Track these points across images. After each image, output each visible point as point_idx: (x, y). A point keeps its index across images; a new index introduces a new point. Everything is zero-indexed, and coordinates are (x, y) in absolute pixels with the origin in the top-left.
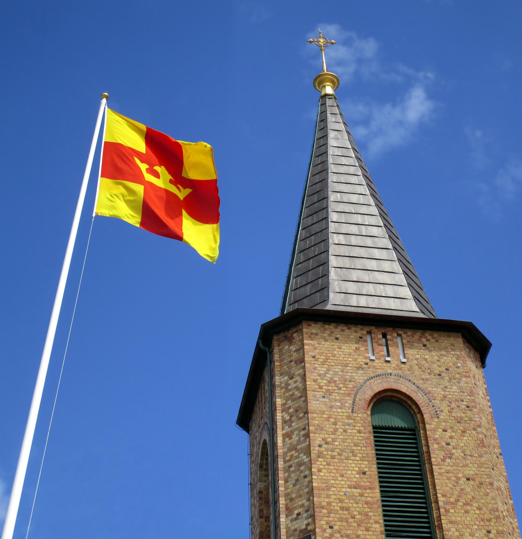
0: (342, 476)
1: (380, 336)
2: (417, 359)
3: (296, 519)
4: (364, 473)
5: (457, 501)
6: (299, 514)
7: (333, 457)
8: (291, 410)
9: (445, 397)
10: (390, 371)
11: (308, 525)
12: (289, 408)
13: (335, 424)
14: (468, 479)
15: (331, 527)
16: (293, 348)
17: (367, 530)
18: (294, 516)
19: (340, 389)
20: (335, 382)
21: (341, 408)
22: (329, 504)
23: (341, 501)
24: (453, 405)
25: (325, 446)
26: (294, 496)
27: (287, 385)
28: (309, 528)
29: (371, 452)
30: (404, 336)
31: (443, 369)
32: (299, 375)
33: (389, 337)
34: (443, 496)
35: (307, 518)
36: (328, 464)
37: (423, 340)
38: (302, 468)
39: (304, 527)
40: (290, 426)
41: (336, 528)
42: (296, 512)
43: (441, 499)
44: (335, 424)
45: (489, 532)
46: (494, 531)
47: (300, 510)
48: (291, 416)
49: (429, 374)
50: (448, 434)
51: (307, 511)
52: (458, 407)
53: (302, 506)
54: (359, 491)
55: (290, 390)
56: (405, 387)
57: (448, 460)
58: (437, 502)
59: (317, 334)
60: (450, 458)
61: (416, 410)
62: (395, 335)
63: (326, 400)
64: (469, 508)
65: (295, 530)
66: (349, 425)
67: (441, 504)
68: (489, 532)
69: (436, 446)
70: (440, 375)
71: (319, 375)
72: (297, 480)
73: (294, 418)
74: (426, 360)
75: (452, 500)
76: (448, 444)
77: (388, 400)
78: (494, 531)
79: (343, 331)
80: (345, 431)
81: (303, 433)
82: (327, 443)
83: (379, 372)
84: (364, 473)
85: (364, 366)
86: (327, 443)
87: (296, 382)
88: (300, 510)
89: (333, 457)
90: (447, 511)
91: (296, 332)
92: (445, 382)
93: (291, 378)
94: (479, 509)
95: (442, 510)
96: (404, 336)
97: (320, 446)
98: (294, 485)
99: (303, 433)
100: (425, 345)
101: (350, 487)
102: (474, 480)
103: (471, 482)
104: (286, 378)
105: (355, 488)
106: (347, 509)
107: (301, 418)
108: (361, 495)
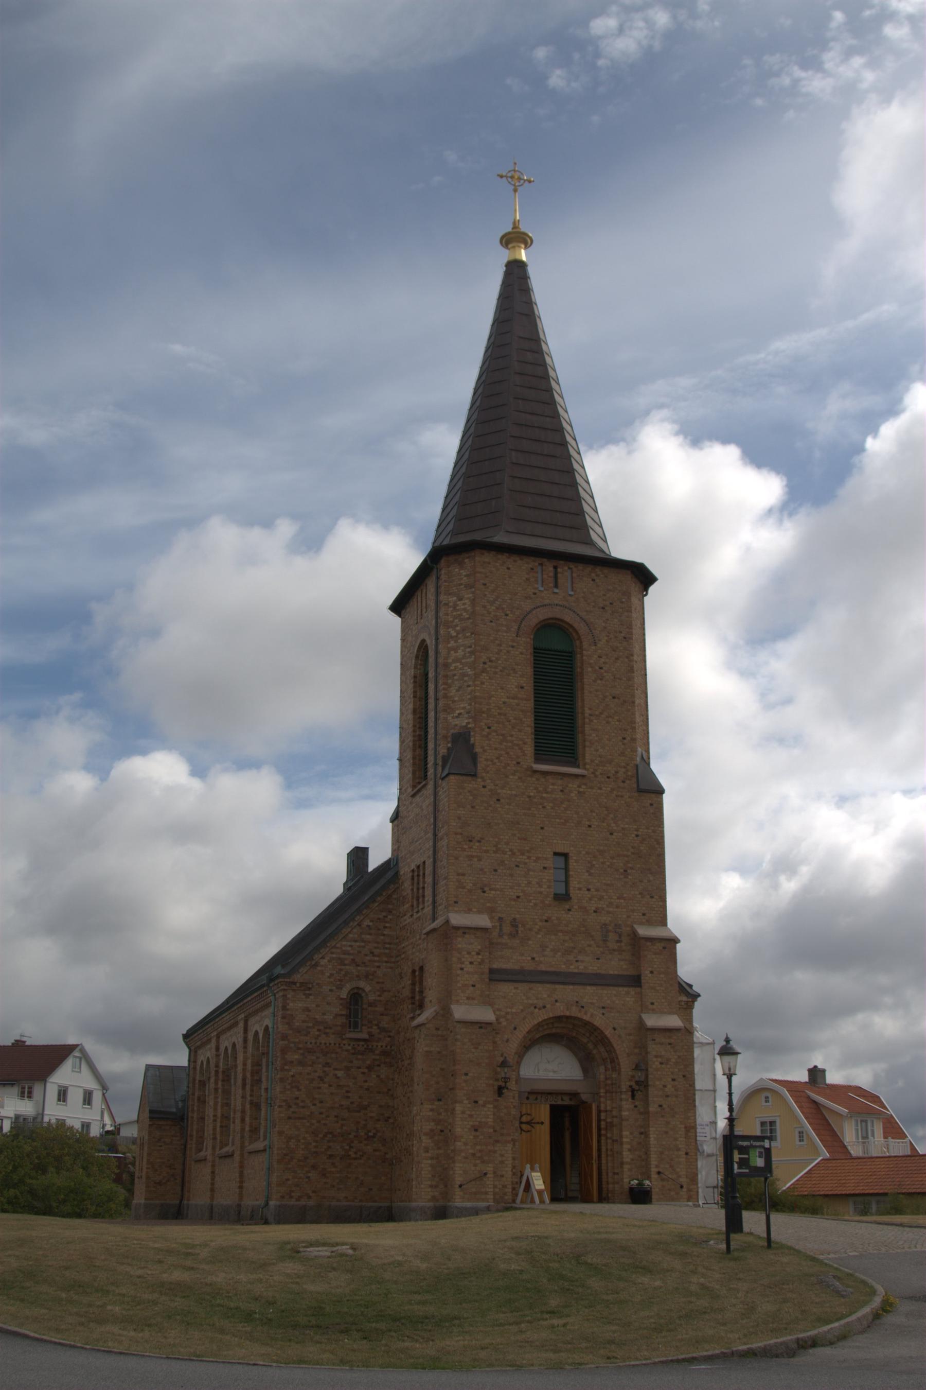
0: (502, 688)
1: (551, 569)
2: (584, 593)
3: (457, 717)
4: (522, 688)
5: (601, 713)
6: (460, 714)
7: (496, 673)
8: (458, 628)
9: (605, 628)
10: (556, 602)
11: (468, 723)
12: (457, 626)
13: (500, 645)
14: (614, 698)
15: (489, 728)
16: (463, 572)
17: (520, 731)
18: (456, 715)
19: (507, 615)
20: (503, 609)
21: (506, 632)
23: (500, 708)
24: (611, 636)
25: (489, 663)
26: (456, 699)
27: (455, 606)
28: (469, 726)
29: (529, 671)
30: (575, 569)
32: (467, 598)
33: (559, 570)
34: (590, 709)
35: (467, 718)
36: (490, 678)
37: (593, 575)
38: (466, 678)
39: (464, 724)
40: (456, 642)
41: (493, 728)
42: (458, 712)
43: (587, 711)
44: (500, 645)
45: (624, 739)
46: (628, 739)
47: (462, 711)
48: (458, 634)
49: (594, 607)
50: (603, 660)
51: (468, 713)
52: (616, 637)
53: (464, 708)
54: (516, 701)
55: (458, 610)
56: (568, 617)
57: (599, 682)
58: (583, 713)
59: (489, 563)
60: (601, 680)
61: (576, 637)
62: (566, 568)
63: (493, 624)
64: (610, 719)
65: (456, 725)
66: (513, 647)
67: (587, 715)
68: (624, 739)
69: (590, 669)
70: (603, 608)
72: (460, 687)
73: (460, 636)
74: (592, 593)
75: (597, 713)
76: (601, 668)
77: (552, 627)
78: (628, 739)
79: (515, 561)
80: (508, 652)
81: (469, 650)
82: (491, 661)
83: (547, 602)
84: (522, 688)
85: (533, 596)
86: (491, 661)
87: (464, 604)
88: (462, 711)
89: (496, 673)
90: (591, 721)
91: (468, 558)
93: (460, 600)
94: (619, 721)
95: (587, 720)
96: (575, 569)
97: (485, 663)
98: (458, 691)
99: (469, 650)
100: (593, 580)
101: (508, 698)
102: (619, 698)
103: (616, 700)
104: (455, 598)
105: (513, 698)
106: (505, 715)
107: (468, 637)
108: (518, 705)
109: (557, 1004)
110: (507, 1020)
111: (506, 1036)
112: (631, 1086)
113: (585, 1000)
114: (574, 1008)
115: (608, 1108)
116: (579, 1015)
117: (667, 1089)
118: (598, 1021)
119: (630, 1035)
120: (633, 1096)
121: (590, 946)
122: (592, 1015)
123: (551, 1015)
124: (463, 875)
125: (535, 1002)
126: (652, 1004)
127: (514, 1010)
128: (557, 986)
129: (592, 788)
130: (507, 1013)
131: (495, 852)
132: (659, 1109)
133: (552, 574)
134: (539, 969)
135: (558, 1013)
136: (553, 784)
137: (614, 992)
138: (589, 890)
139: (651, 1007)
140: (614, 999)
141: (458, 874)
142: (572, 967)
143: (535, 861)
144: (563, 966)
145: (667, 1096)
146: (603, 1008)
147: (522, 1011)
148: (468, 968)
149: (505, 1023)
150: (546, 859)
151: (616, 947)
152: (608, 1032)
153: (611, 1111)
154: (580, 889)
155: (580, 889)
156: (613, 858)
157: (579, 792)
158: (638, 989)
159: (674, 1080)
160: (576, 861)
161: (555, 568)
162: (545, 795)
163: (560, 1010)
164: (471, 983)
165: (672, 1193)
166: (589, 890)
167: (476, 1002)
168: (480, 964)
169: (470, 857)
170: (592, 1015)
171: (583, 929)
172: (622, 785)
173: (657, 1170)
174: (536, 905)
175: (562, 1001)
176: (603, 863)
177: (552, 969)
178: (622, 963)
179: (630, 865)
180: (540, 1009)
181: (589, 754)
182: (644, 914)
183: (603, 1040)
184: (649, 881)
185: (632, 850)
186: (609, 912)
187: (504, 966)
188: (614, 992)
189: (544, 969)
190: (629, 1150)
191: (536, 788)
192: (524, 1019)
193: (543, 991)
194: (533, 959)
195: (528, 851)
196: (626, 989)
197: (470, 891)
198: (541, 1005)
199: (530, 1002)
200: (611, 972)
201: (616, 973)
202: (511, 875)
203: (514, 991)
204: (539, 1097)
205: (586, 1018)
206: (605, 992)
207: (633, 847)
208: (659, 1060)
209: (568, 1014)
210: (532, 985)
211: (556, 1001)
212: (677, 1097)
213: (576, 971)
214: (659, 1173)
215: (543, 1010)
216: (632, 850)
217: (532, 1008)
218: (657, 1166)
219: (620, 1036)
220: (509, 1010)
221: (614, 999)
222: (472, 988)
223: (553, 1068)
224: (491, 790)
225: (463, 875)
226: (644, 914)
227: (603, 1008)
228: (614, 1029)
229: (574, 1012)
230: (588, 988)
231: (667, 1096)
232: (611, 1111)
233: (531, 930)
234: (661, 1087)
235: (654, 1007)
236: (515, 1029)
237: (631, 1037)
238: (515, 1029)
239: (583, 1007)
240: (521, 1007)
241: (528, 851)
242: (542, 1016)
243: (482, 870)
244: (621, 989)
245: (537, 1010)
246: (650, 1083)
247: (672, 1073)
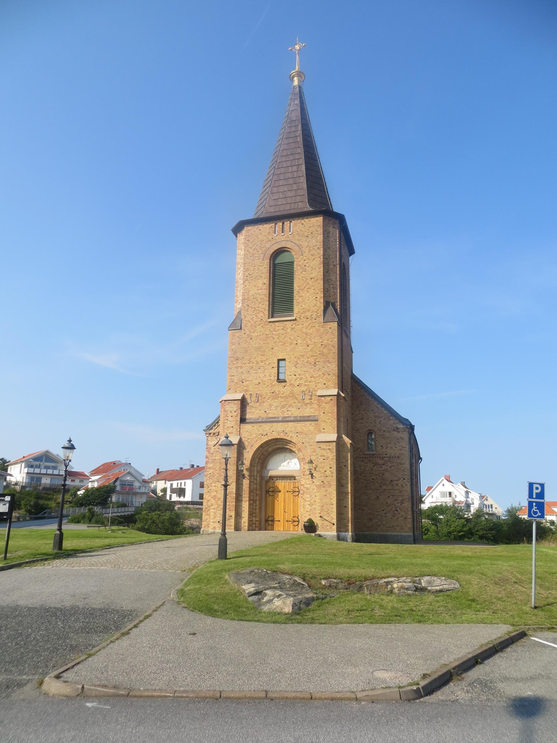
22: (248, 298)
23: (253, 296)
31: (310, 233)
71: (250, 248)
83: (278, 240)
92: (310, 239)
114: (282, 434)
117: (326, 473)
121: (295, 403)
122: (291, 437)
124: (234, 376)
126: (324, 429)
129: (298, 325)
130: (249, 439)
131: (249, 363)
132: (322, 483)
133: (281, 227)
136: (278, 327)
138: (295, 375)
139: (323, 430)
141: (231, 376)
143: (268, 365)
145: (327, 476)
148: (230, 419)
150: (274, 363)
151: (308, 402)
154: (291, 375)
155: (291, 375)
156: (308, 358)
157: (292, 328)
159: (331, 468)
160: (289, 362)
161: (283, 224)
162: (274, 333)
163: (275, 436)
165: (328, 527)
166: (295, 375)
169: (237, 367)
170: (291, 437)
171: (291, 395)
172: (314, 321)
173: (320, 515)
174: (268, 386)
176: (303, 361)
179: (317, 360)
181: (296, 309)
182: (325, 384)
184: (328, 367)
185: (319, 352)
186: (306, 385)
190: (309, 505)
191: (270, 330)
193: (267, 427)
195: (265, 361)
197: (236, 383)
202: (256, 373)
207: (320, 351)
208: (323, 457)
212: (332, 476)
214: (321, 517)
216: (319, 352)
218: (320, 513)
219: (306, 447)
224: (248, 335)
225: (234, 376)
226: (325, 384)
229: (282, 436)
231: (327, 476)
233: (265, 398)
234: (323, 471)
235: (325, 430)
241: (265, 361)
242: (265, 439)
243: (242, 372)
247: (330, 464)
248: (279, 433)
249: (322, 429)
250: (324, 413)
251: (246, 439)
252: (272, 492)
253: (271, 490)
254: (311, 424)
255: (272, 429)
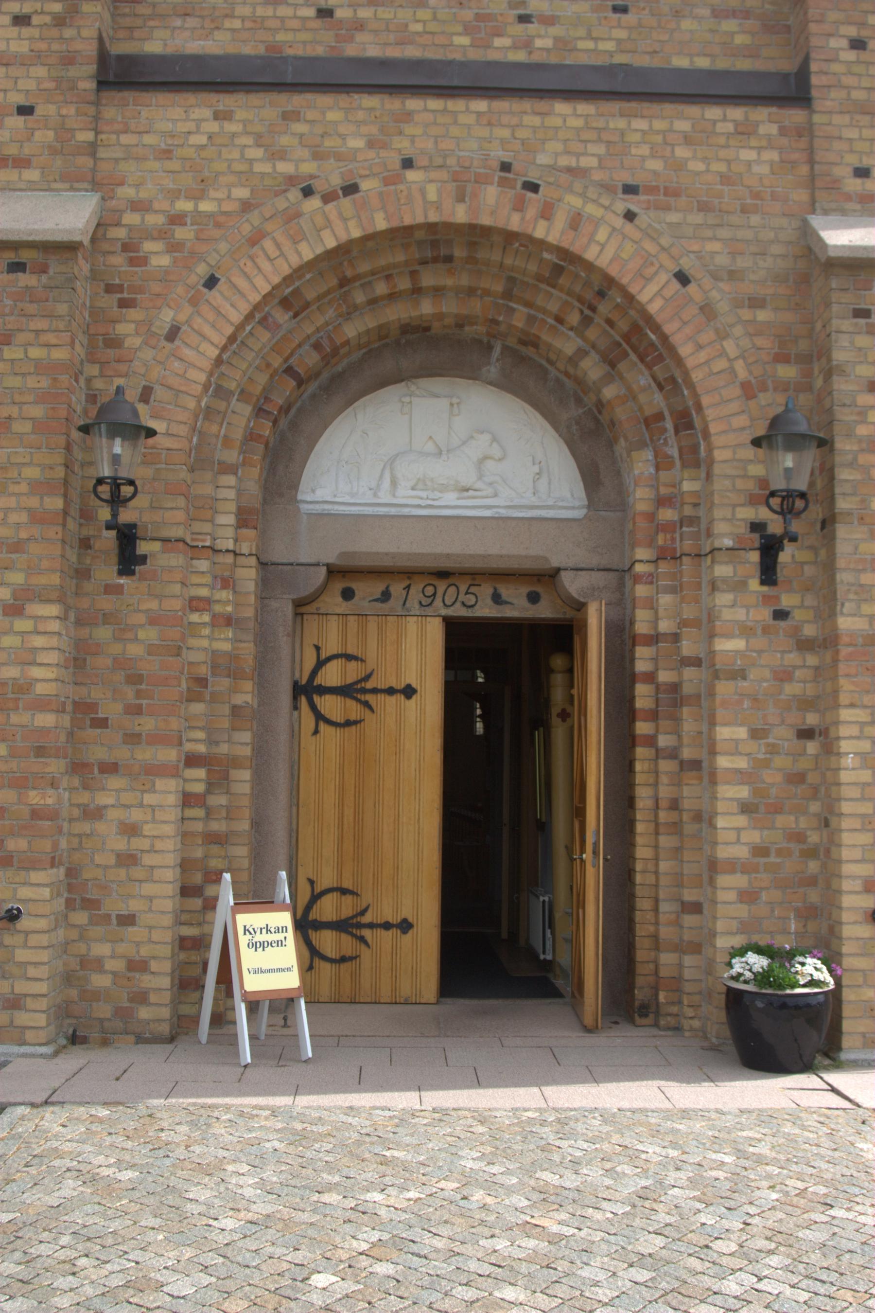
109: (411, 175)
110: (174, 247)
111: (167, 316)
112: (757, 527)
113: (543, 159)
114: (491, 193)
115: (664, 626)
116: (515, 223)
118: (606, 247)
119: (756, 303)
120: (768, 573)
122: (576, 221)
123: (381, 224)
125: (309, 168)
126: (862, 173)
127: (205, 206)
128: (413, 104)
130: (177, 219)
134: (351, 51)
135: (415, 215)
137: (683, 126)
139: (854, 185)
140: (681, 152)
142: (498, 42)
144: (465, 41)
146: (630, 190)
147: (246, 206)
149: (165, 261)
152: (653, 294)
153: (676, 638)
158: (795, 116)
163: (427, 199)
164: (19, 99)
167: (32, 175)
168: (60, 21)
175: (433, 164)
177: (411, 52)
178: (729, 25)
180: (327, 198)
183: (639, 340)
187: (195, 46)
188: (683, 126)
189: (373, 52)
192: (256, 239)
193: (347, 126)
194: (325, 13)
196: (737, 113)
198: (336, 181)
199: (285, 168)
200: (681, 62)
201: (703, 63)
203: (213, 127)
204: (397, 589)
205: (550, 231)
206: (640, 124)
209: (461, 215)
210: (297, 100)
211: (408, 163)
213: (520, 56)
215: (346, 203)
217: (294, 195)
219: (707, 310)
220: (184, 205)
221: (681, 152)
222: (19, 121)
223: (445, 469)
227: (630, 190)
228: (683, 278)
229: (493, 206)
230: (561, 107)
232: (676, 638)
236: (211, 282)
237: (762, 316)
238: (211, 282)
239: (533, 187)
240: (242, 193)
242: (340, 225)
244: (713, 112)
245: (315, 203)
246: (842, 504)
248: (463, 184)
249: (843, 172)
250: (858, 44)
251: (155, 220)
252: (345, 691)
253: (331, 675)
254: (744, 131)
255: (403, 145)
